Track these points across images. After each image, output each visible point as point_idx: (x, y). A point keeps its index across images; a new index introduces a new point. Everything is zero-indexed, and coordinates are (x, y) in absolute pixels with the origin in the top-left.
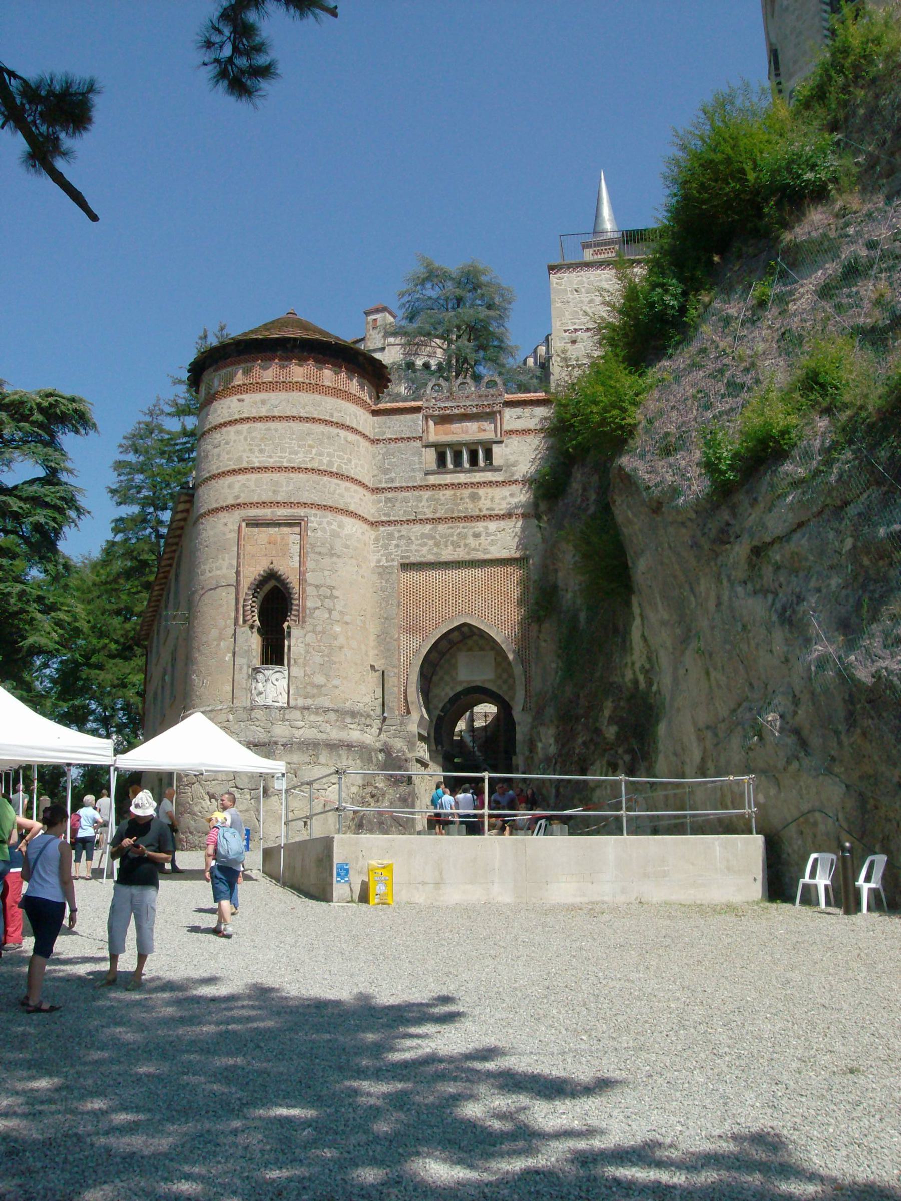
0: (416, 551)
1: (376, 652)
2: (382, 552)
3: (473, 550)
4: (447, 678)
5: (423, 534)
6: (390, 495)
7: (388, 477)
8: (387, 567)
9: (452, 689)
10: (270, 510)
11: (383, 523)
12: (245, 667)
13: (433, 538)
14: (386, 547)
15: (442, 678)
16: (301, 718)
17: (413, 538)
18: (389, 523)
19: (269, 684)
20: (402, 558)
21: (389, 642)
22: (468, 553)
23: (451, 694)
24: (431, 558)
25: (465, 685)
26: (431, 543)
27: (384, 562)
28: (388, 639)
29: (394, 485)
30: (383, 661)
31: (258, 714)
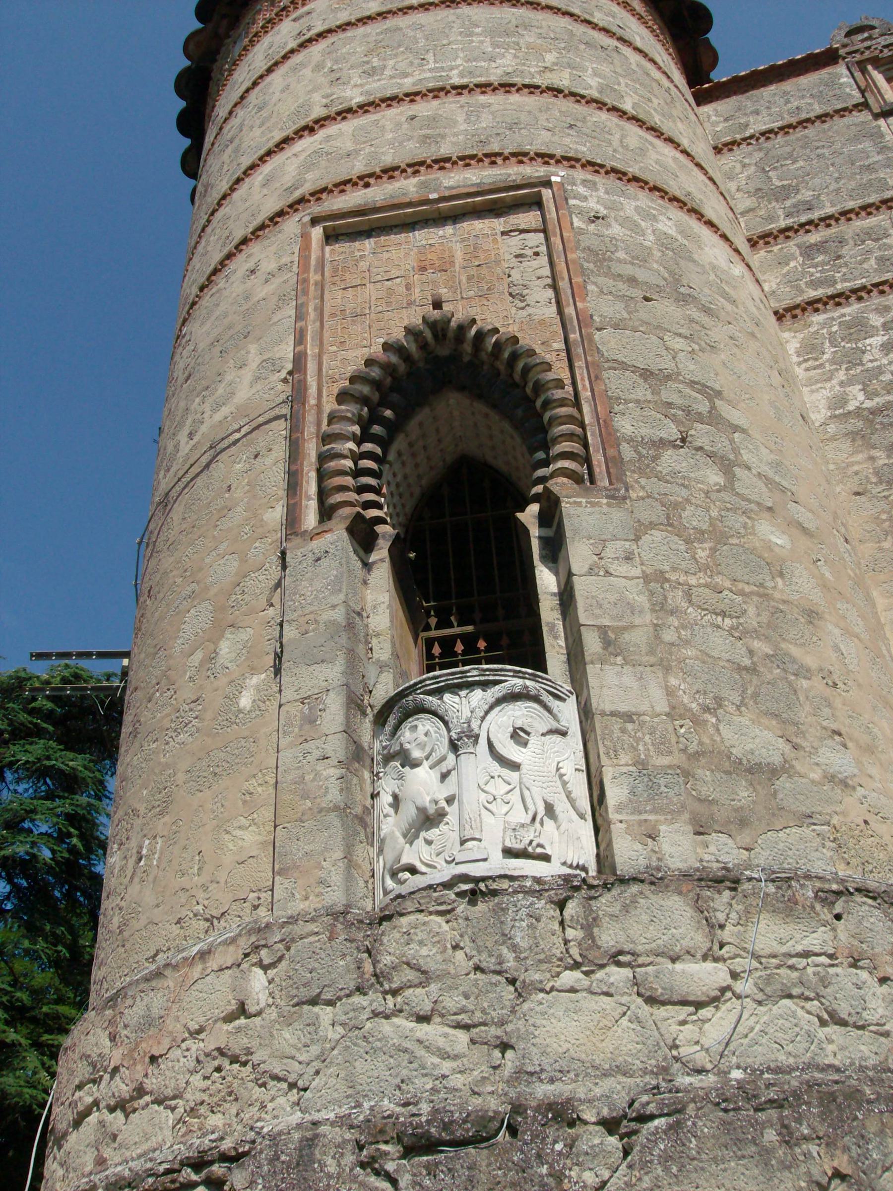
2: (841, 375)
6: (814, 238)
7: (788, 203)
8: (873, 412)
10: (414, 180)
11: (814, 305)
12: (335, 704)
14: (853, 359)
16: (699, 940)
18: (838, 299)
19: (476, 765)
27: (857, 398)
29: (815, 215)
31: (421, 939)
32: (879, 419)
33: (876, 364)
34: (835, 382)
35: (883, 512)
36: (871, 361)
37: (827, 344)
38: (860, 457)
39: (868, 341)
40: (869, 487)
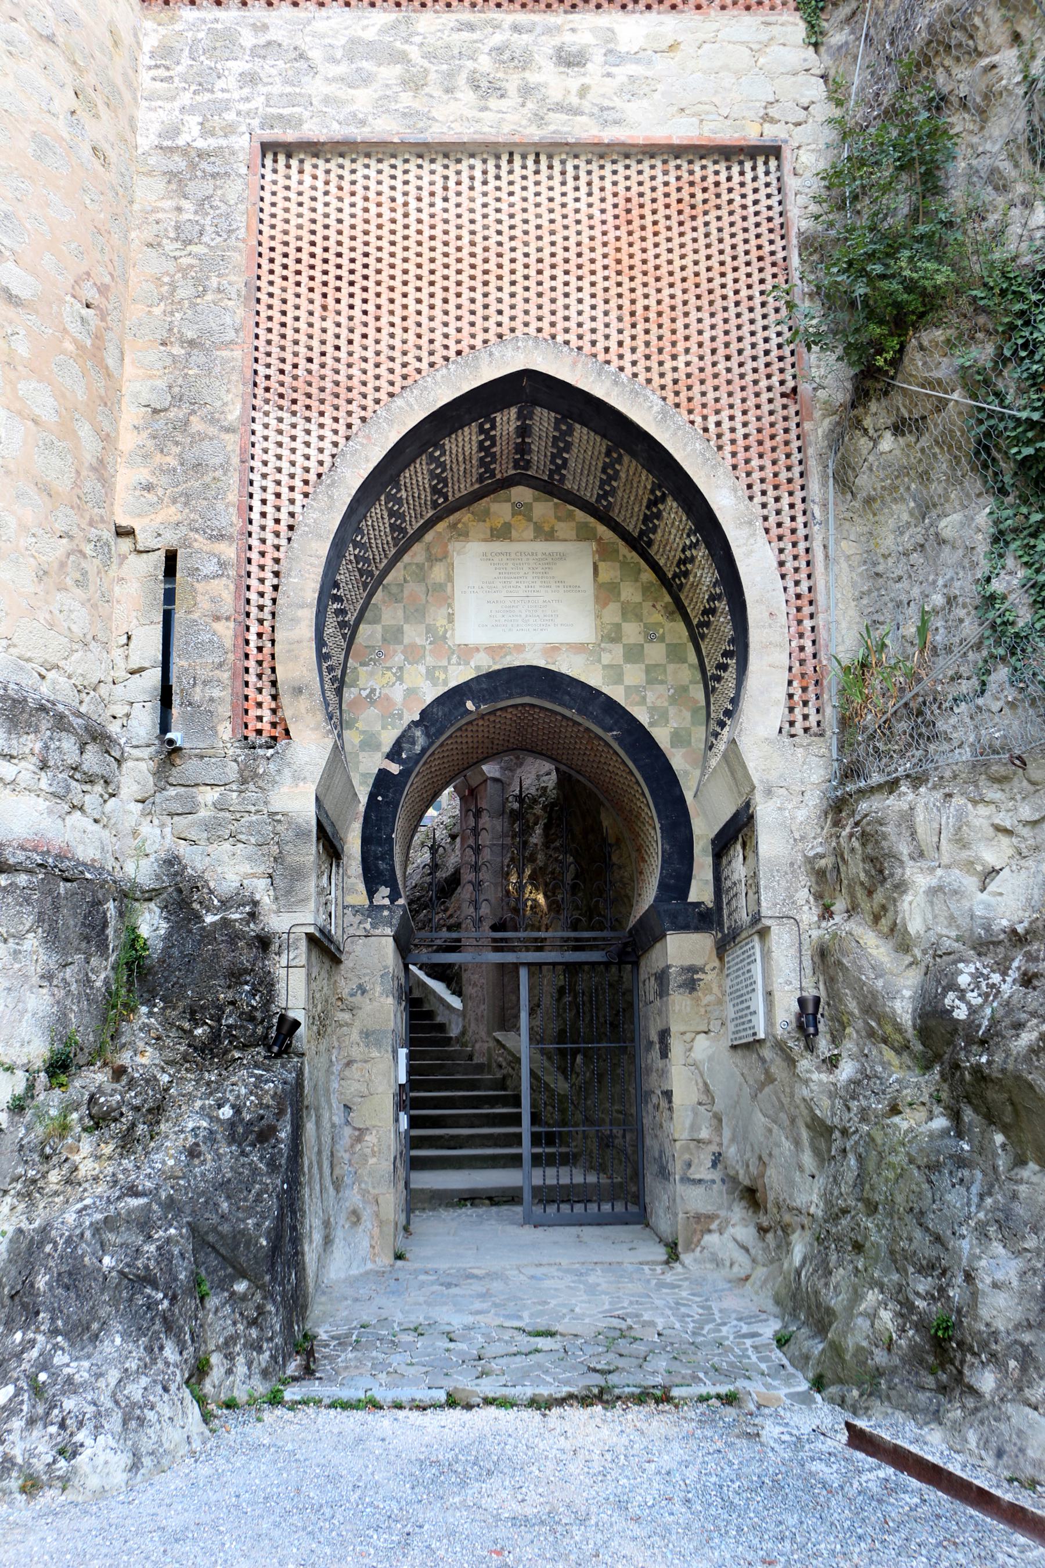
0: (327, 100)
1: (144, 475)
2: (186, 99)
3: (559, 108)
4: (413, 634)
5: (353, 41)
9: (430, 674)
13: (402, 58)
15: (394, 635)
17: (316, 55)
20: (268, 122)
21: (202, 437)
22: (539, 119)
23: (430, 694)
24: (385, 127)
25: (486, 664)
26: (391, 73)
27: (191, 134)
28: (197, 425)
30: (172, 512)
32: (203, 165)
33: (226, 96)
34: (177, 104)
35: (167, 273)
36: (223, 90)
37: (186, 53)
38: (168, 204)
39: (230, 64)
40: (165, 241)
